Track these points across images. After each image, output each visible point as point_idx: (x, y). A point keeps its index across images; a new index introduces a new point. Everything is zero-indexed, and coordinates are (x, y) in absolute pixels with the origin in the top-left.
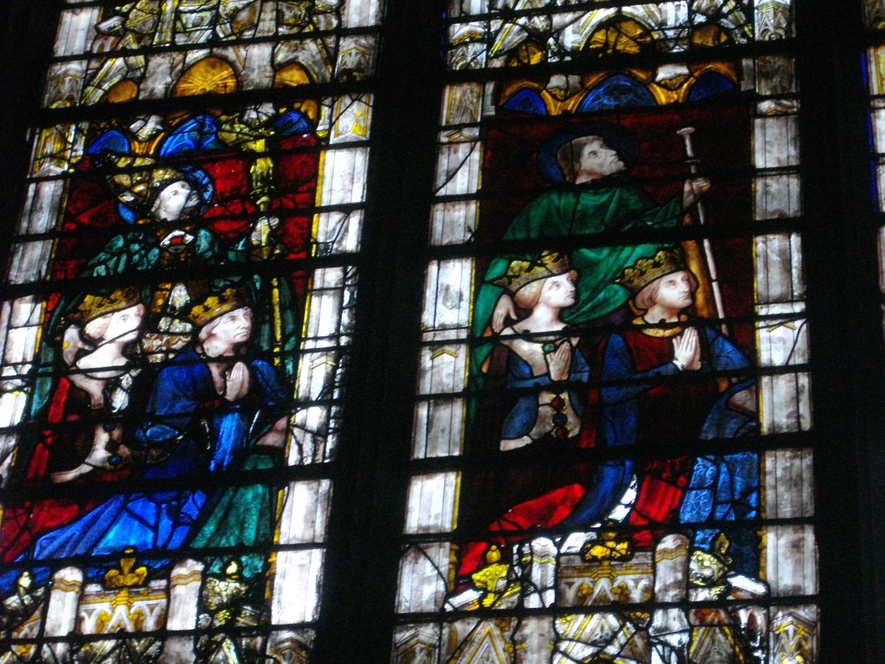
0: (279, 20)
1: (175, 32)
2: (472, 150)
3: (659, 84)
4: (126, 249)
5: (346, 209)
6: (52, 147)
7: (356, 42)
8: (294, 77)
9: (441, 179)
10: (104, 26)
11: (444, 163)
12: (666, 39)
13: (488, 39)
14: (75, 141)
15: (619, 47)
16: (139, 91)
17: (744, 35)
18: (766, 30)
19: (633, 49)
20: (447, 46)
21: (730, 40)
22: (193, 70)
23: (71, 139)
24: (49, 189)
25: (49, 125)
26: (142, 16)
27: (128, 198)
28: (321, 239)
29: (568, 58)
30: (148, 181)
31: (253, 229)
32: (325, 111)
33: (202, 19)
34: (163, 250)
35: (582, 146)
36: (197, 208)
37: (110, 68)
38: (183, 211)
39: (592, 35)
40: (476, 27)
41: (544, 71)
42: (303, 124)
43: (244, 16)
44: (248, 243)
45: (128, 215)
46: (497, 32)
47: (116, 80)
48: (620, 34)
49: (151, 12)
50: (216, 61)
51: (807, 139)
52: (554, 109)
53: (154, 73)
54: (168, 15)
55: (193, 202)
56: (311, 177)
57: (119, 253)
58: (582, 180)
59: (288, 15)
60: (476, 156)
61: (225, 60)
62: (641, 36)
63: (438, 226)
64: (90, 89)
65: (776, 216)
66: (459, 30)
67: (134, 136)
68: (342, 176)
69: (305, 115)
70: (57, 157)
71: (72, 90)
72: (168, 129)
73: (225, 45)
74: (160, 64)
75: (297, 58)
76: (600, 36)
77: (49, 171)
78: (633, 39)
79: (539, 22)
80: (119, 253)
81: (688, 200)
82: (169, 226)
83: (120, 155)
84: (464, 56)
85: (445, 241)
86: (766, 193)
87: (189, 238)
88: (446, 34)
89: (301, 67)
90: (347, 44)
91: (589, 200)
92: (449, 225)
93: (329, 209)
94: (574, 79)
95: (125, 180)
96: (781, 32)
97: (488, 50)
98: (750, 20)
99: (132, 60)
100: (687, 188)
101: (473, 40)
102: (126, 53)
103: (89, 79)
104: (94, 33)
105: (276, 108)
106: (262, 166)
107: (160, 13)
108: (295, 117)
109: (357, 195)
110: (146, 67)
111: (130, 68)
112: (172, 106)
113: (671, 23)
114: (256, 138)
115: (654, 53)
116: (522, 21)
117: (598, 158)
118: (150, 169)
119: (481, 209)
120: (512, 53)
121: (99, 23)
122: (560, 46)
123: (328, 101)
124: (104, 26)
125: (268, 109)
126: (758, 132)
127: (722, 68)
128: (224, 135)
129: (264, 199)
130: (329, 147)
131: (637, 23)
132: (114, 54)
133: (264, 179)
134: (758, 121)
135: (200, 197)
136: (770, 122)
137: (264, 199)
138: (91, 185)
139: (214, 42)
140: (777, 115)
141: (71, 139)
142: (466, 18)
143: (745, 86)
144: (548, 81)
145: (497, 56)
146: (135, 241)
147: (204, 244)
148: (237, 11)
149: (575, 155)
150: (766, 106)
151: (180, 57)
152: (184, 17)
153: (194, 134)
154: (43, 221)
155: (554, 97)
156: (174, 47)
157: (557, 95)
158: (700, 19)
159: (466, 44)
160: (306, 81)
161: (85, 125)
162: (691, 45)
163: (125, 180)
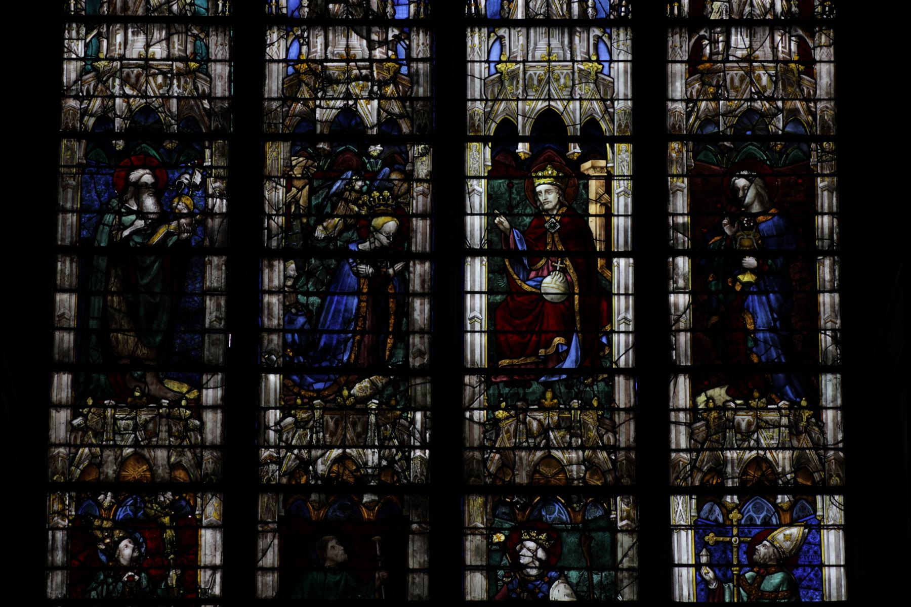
0: (170, 434)
1: (115, 433)
2: (274, 538)
3: (364, 505)
4: (104, 582)
5: (214, 568)
6: (57, 506)
7: (211, 454)
8: (181, 475)
9: (260, 554)
10: (75, 422)
11: (261, 544)
12: (368, 475)
13: (279, 462)
14: (69, 505)
15: (345, 477)
16: (100, 473)
17: (406, 478)
18: (416, 476)
19: (352, 480)
20: (258, 463)
21: (399, 481)
22: (127, 462)
23: (67, 503)
24: (59, 535)
25: (54, 493)
26: (96, 418)
27: (102, 547)
28: (203, 586)
29: (319, 482)
30: (111, 536)
31: (169, 575)
32: (199, 500)
33: (128, 425)
34: (124, 583)
35: (328, 541)
36: (138, 557)
37: (82, 454)
38: (132, 559)
39: (331, 467)
40: (272, 451)
41: (308, 489)
42: (188, 509)
43: (151, 425)
44: (167, 584)
45: (103, 558)
46: (284, 457)
47: (86, 463)
48: (345, 468)
49: (99, 416)
50: (138, 457)
51: (432, 551)
52: (313, 514)
53: (106, 462)
54: (110, 421)
55: (135, 554)
56: (194, 545)
57: (101, 583)
58: (328, 564)
59: (174, 429)
60: (276, 541)
61: (143, 456)
62: (356, 471)
63: (260, 585)
64: (73, 468)
65: (417, 599)
66: (265, 453)
67: (100, 505)
68: (210, 545)
69: (188, 502)
70: (62, 514)
71: (63, 468)
72: (118, 502)
73: (143, 447)
74: (109, 455)
75: (181, 461)
76: (335, 468)
77: (58, 523)
78: (351, 472)
79: (304, 453)
80: (101, 583)
81: (377, 583)
82: (126, 569)
83: (95, 517)
84: (267, 472)
85: (264, 596)
86: (413, 583)
87: (137, 577)
88: (258, 455)
89: (184, 469)
90: (207, 455)
91: (332, 578)
92: (265, 584)
93: (206, 567)
94: (323, 496)
95: (98, 533)
96: (423, 478)
97: (279, 470)
98: (409, 468)
99: (93, 450)
100: (377, 575)
101: (272, 462)
102: (90, 446)
103: (71, 460)
104: (70, 427)
105: (172, 495)
106: (169, 534)
107: (105, 417)
108: (184, 503)
109: (218, 561)
110: (101, 455)
111: (93, 455)
112: (119, 486)
113: (370, 464)
114: (165, 516)
115: (361, 484)
116: (296, 451)
117: (336, 551)
118: (111, 530)
119: (279, 576)
120: (291, 474)
121: (72, 420)
122: (315, 471)
123: (199, 495)
124: (75, 422)
125: (169, 495)
126: (410, 542)
127: (395, 499)
128: (148, 510)
129: (172, 556)
130: (202, 527)
131: (354, 461)
132: (83, 445)
133: (171, 543)
134: (411, 536)
135: (140, 551)
136: (416, 537)
137: (172, 556)
138: (81, 534)
139: (136, 444)
140: (420, 533)
141: (67, 503)
142: (268, 447)
143: (405, 513)
144: (310, 496)
145: (284, 475)
146: (109, 576)
147: (144, 582)
148: (146, 422)
149: (325, 548)
150: (415, 526)
151: (119, 452)
152: (119, 422)
153: (132, 507)
154: (59, 557)
155: (313, 507)
156: (115, 446)
157: (315, 509)
158: (384, 463)
159: (268, 464)
160: (187, 479)
161: (73, 494)
162: (380, 480)
163: (98, 533)
